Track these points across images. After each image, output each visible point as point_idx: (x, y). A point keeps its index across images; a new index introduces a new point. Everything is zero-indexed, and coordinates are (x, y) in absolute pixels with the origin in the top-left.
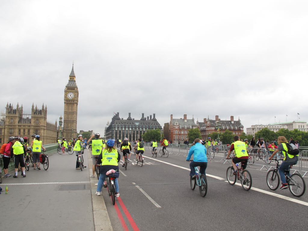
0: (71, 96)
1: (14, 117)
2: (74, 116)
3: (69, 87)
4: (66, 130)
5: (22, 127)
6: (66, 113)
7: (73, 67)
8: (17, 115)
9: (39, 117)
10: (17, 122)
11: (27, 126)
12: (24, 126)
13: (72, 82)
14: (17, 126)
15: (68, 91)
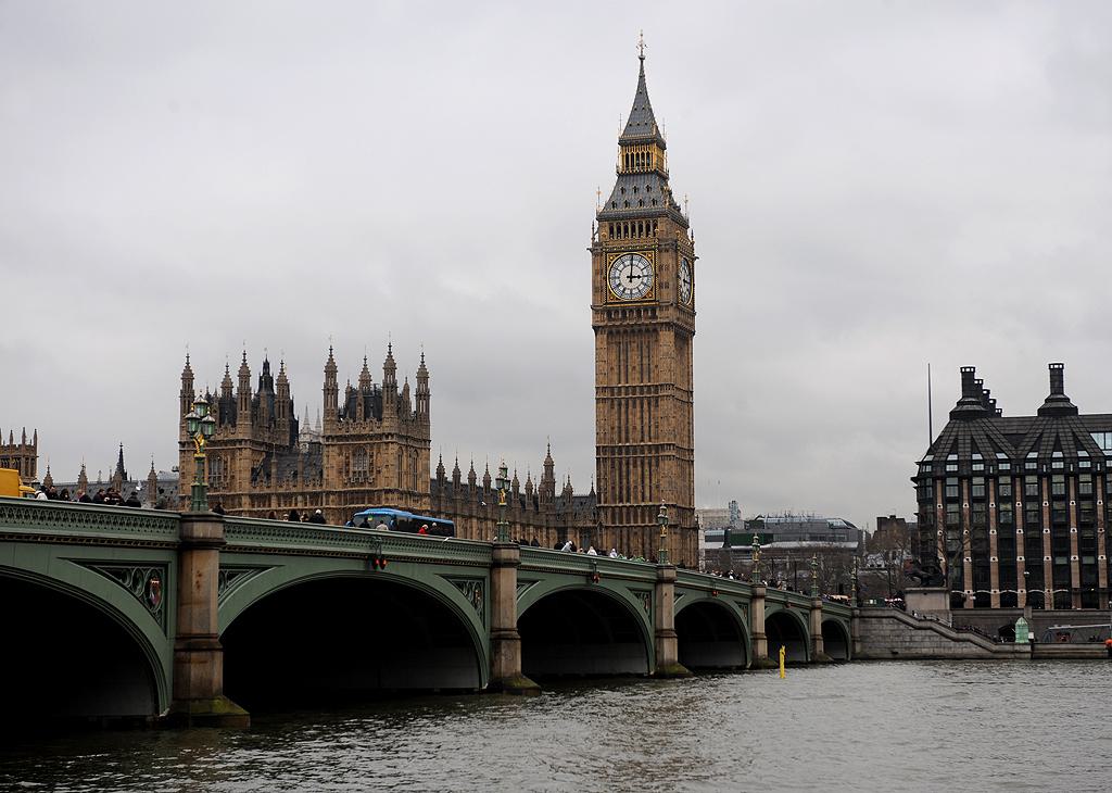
0: (633, 278)
1: (226, 443)
2: (660, 414)
3: (617, 218)
4: (616, 513)
5: (274, 506)
6: (609, 397)
7: (642, 77)
8: (243, 431)
9: (371, 437)
10: (247, 475)
11: (303, 494)
12: (288, 497)
13: (642, 183)
14: (246, 500)
15: (616, 243)
